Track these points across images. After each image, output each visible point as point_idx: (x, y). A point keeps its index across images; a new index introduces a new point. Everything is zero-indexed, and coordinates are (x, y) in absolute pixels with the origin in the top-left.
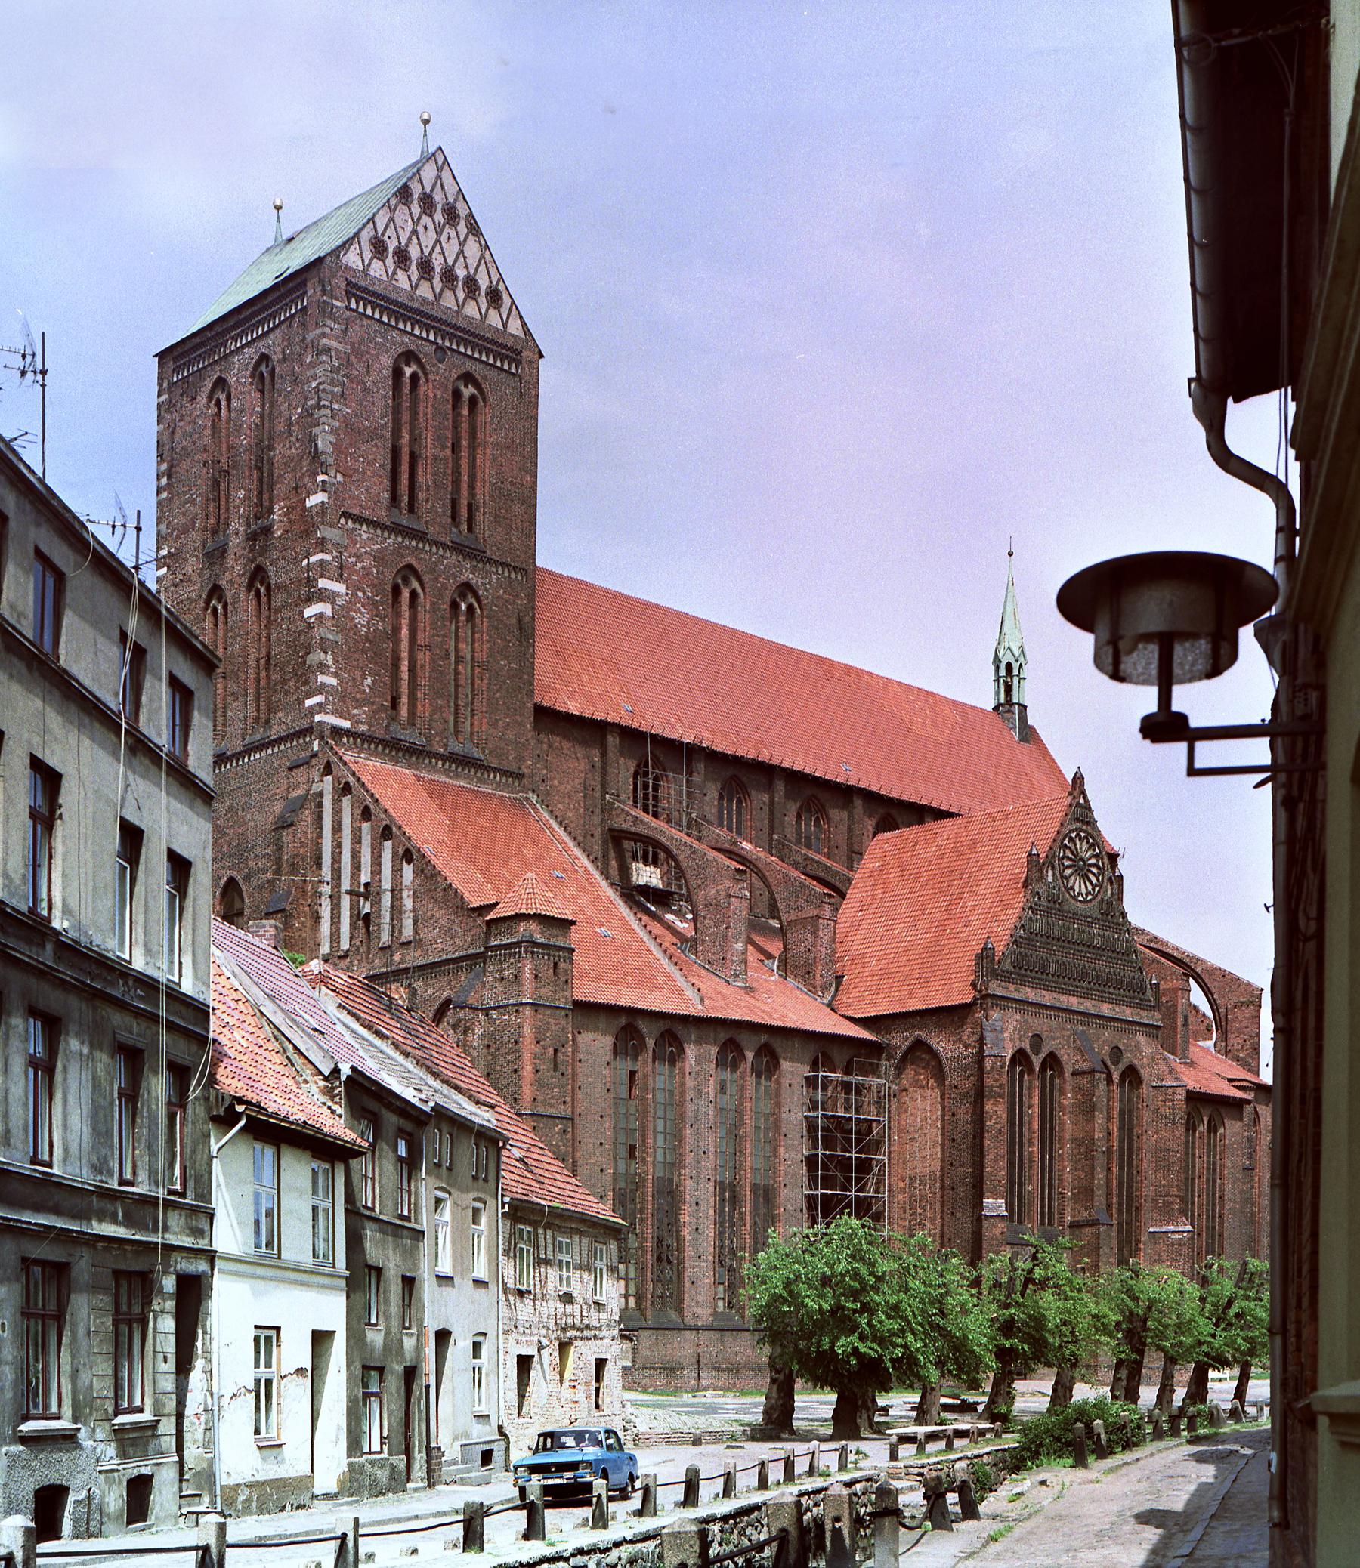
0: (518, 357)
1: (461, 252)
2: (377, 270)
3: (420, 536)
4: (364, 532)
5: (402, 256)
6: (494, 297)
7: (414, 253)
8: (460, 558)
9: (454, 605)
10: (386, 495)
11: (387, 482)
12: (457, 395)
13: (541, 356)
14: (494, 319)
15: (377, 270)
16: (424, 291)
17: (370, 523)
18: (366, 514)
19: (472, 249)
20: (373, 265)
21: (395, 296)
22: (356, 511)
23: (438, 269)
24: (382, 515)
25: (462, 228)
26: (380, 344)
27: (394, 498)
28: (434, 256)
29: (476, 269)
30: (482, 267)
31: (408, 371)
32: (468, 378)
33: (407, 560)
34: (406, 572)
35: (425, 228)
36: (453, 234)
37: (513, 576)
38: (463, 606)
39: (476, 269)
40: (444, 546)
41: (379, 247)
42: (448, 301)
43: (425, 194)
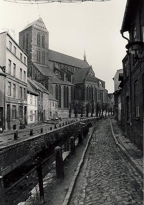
0: (47, 33)
2: (36, 27)
4: (35, 46)
6: (45, 29)
10: (37, 44)
15: (36, 27)
24: (37, 45)
27: (38, 44)
32: (43, 35)
41: (36, 25)
43: (40, 21)
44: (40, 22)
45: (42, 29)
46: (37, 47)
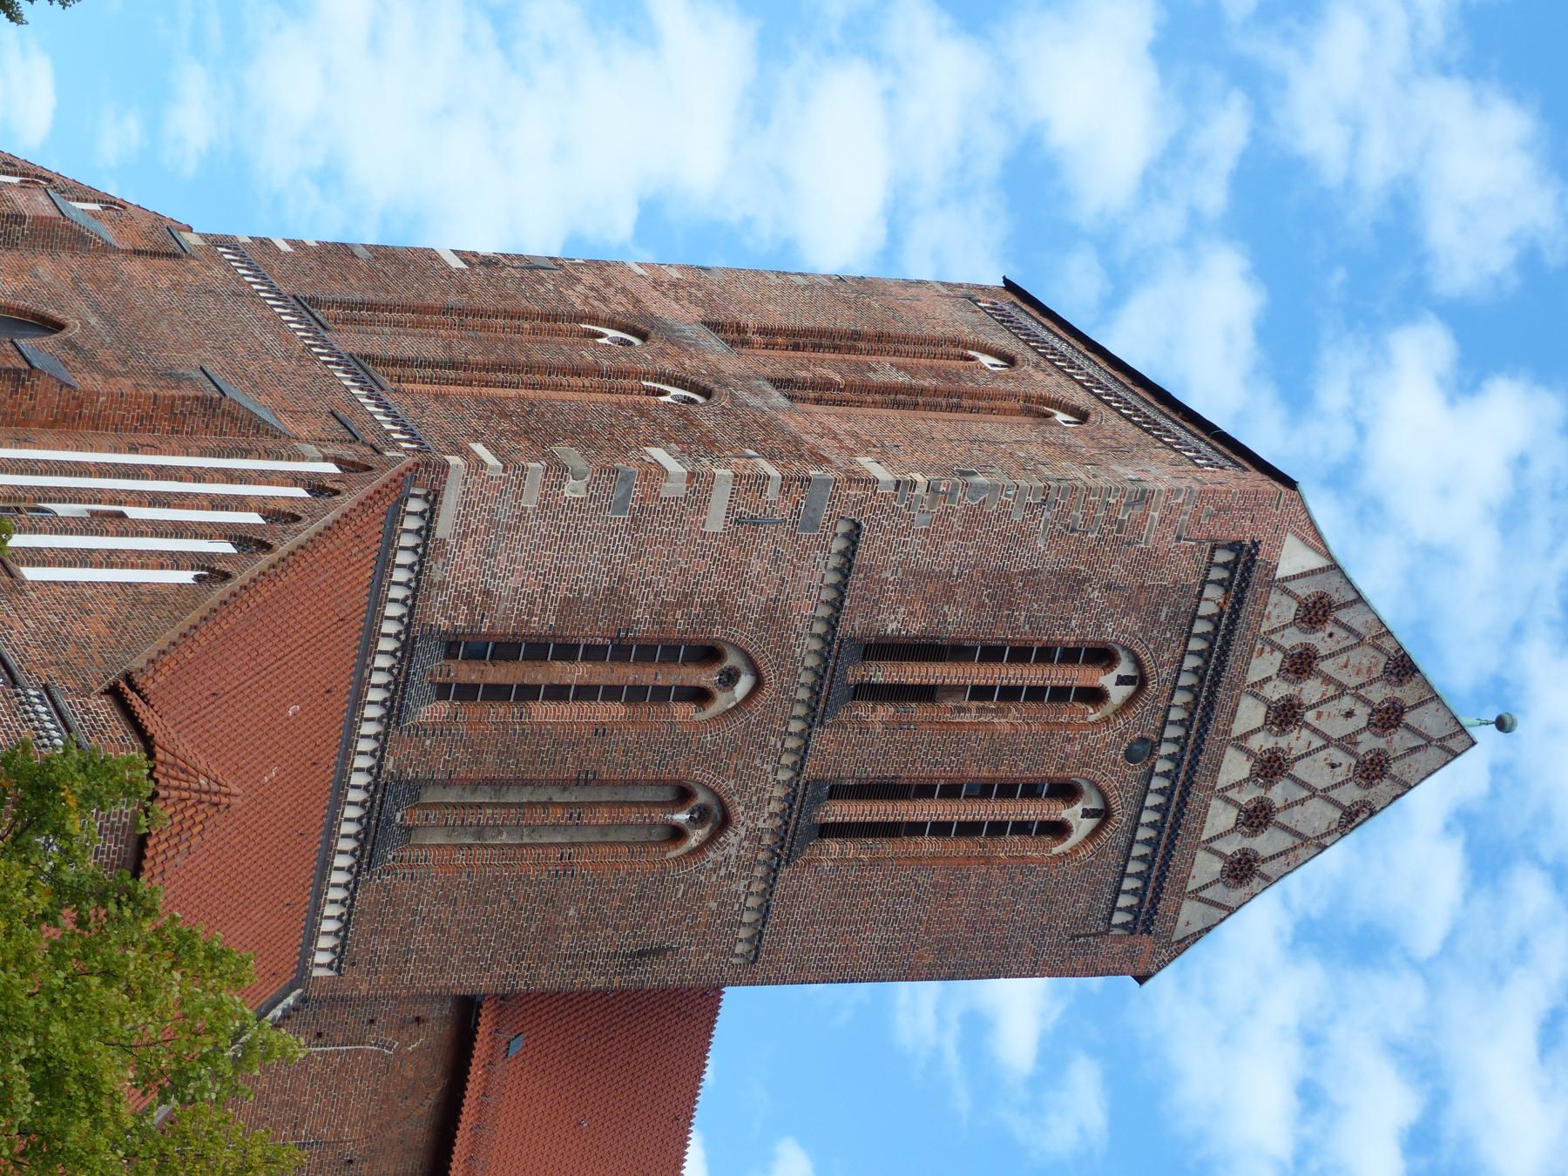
1: (1314, 793)
2: (1281, 610)
3: (815, 715)
5: (1301, 664)
6: (1243, 872)
7: (1311, 690)
8: (775, 807)
9: (683, 795)
10: (892, 625)
11: (916, 628)
12: (1066, 792)
13: (1141, 979)
14: (1206, 868)
15: (1281, 610)
16: (1250, 714)
17: (841, 588)
18: (857, 580)
19: (1317, 816)
20: (1286, 600)
21: (1237, 647)
22: (864, 555)
23: (1283, 742)
25: (1350, 794)
26: (1157, 612)
28: (1305, 733)
29: (1284, 828)
30: (1285, 841)
31: (1107, 680)
33: (771, 676)
34: (743, 686)
35: (1349, 714)
36: (1341, 774)
37: (744, 933)
38: (682, 817)
39: (1284, 828)
40: (798, 768)
42: (1235, 767)
43: (1400, 723)
44: (1388, 718)
45: (1235, 767)
46: (807, 649)
